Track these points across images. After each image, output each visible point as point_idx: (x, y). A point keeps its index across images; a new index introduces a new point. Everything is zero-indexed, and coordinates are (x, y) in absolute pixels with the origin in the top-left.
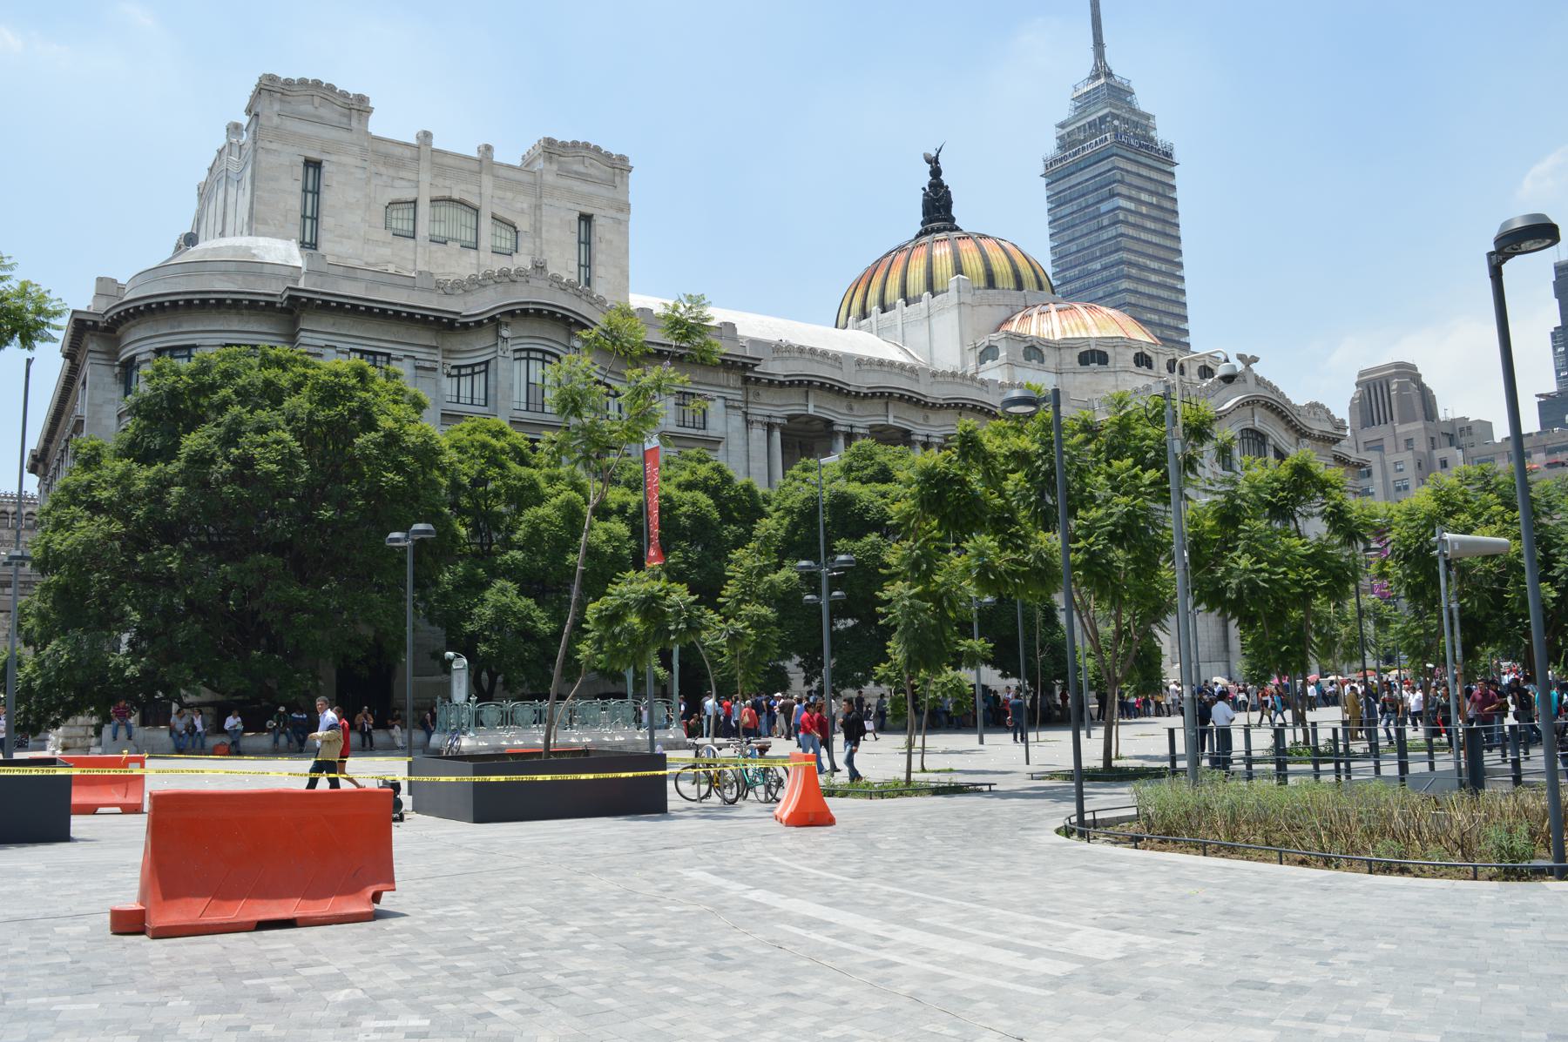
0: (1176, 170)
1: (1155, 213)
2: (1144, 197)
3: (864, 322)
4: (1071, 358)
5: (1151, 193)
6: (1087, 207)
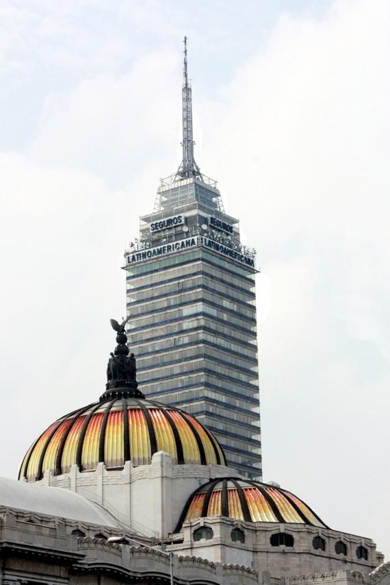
0: (255, 277)
1: (235, 320)
2: (226, 303)
3: (60, 477)
4: (264, 541)
5: (233, 300)
6: (169, 307)
